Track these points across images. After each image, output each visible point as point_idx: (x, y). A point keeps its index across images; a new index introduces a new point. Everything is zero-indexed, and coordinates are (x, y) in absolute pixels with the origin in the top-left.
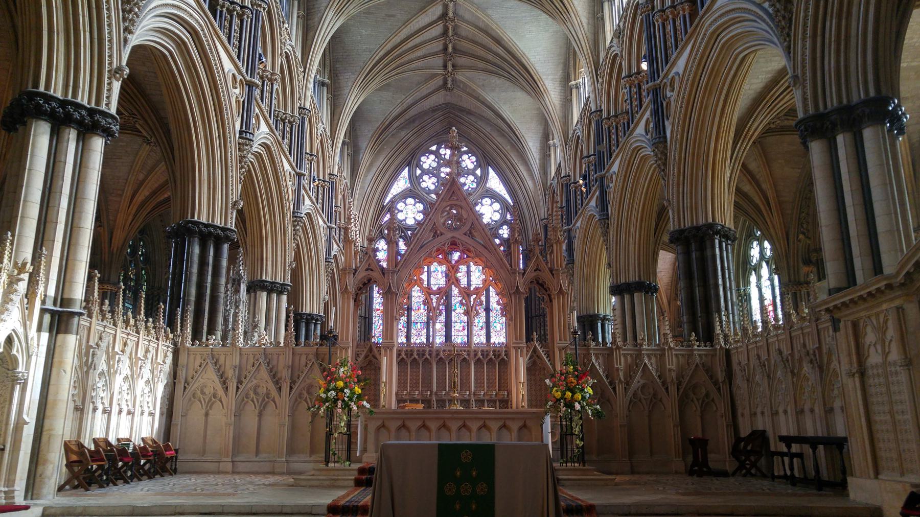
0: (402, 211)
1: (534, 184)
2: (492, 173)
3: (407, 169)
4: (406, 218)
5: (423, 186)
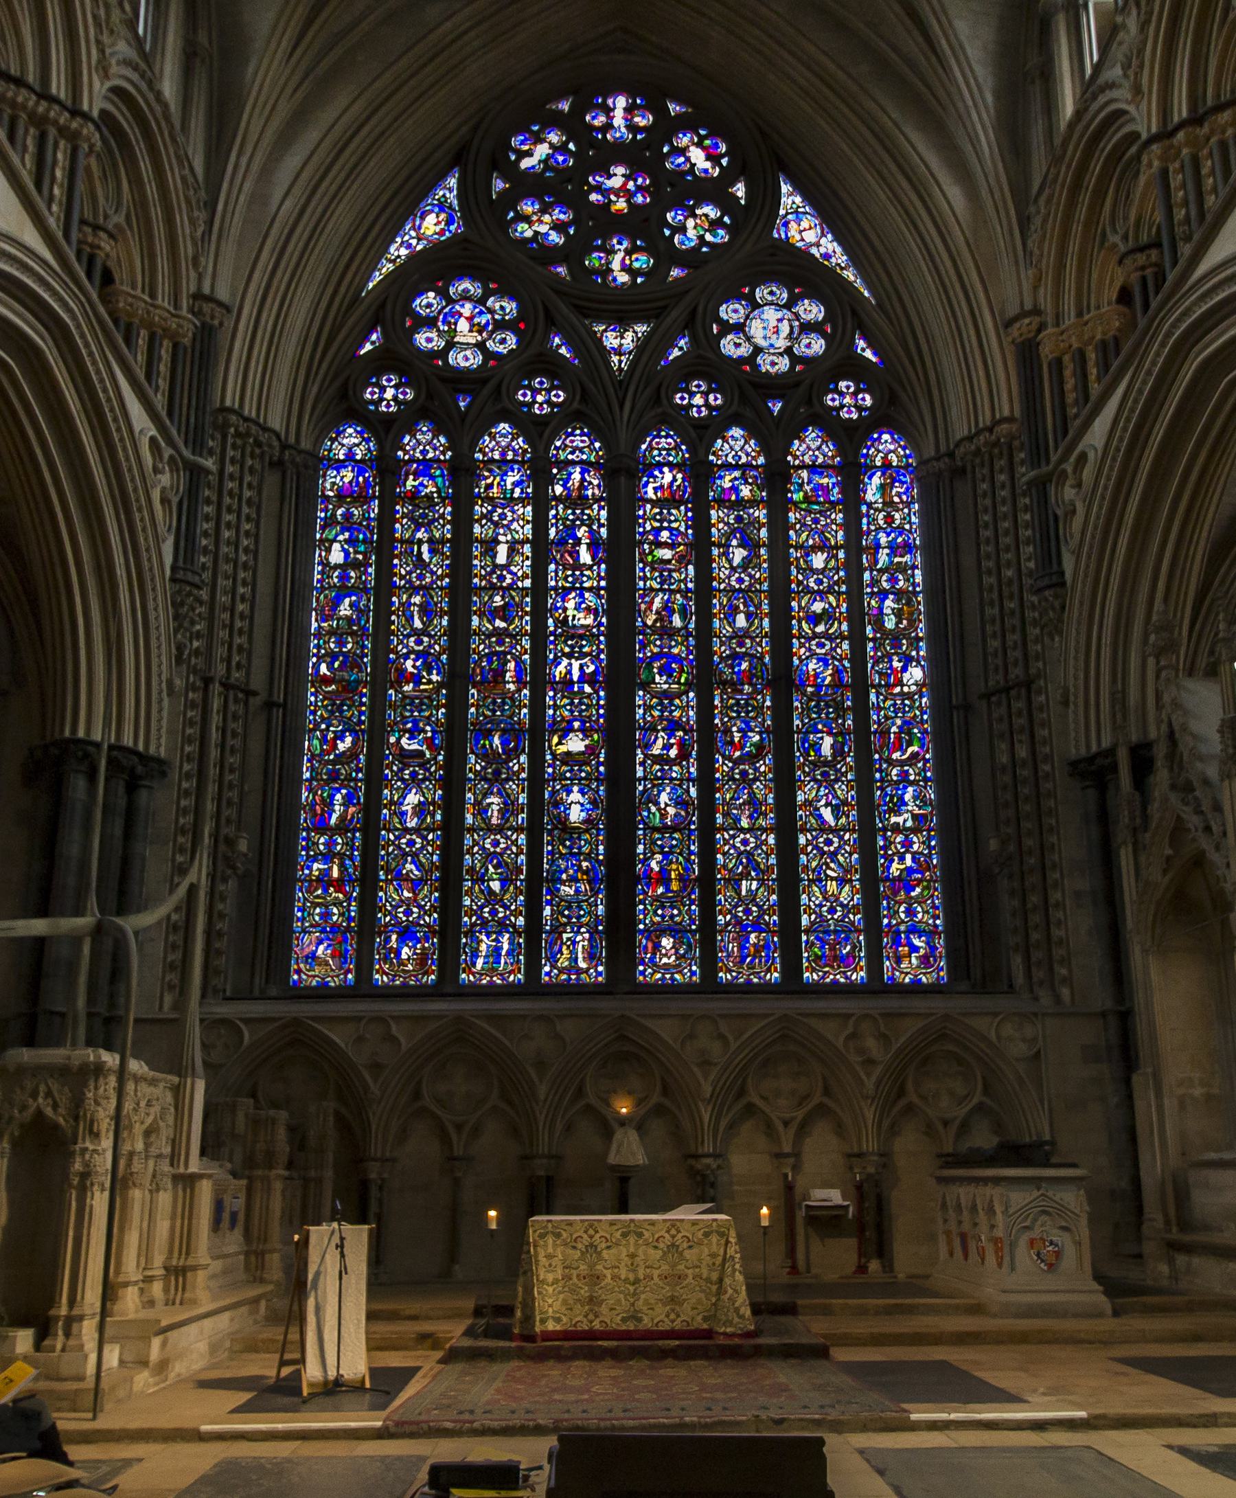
1: (972, 194)
2: (789, 198)
4: (450, 345)
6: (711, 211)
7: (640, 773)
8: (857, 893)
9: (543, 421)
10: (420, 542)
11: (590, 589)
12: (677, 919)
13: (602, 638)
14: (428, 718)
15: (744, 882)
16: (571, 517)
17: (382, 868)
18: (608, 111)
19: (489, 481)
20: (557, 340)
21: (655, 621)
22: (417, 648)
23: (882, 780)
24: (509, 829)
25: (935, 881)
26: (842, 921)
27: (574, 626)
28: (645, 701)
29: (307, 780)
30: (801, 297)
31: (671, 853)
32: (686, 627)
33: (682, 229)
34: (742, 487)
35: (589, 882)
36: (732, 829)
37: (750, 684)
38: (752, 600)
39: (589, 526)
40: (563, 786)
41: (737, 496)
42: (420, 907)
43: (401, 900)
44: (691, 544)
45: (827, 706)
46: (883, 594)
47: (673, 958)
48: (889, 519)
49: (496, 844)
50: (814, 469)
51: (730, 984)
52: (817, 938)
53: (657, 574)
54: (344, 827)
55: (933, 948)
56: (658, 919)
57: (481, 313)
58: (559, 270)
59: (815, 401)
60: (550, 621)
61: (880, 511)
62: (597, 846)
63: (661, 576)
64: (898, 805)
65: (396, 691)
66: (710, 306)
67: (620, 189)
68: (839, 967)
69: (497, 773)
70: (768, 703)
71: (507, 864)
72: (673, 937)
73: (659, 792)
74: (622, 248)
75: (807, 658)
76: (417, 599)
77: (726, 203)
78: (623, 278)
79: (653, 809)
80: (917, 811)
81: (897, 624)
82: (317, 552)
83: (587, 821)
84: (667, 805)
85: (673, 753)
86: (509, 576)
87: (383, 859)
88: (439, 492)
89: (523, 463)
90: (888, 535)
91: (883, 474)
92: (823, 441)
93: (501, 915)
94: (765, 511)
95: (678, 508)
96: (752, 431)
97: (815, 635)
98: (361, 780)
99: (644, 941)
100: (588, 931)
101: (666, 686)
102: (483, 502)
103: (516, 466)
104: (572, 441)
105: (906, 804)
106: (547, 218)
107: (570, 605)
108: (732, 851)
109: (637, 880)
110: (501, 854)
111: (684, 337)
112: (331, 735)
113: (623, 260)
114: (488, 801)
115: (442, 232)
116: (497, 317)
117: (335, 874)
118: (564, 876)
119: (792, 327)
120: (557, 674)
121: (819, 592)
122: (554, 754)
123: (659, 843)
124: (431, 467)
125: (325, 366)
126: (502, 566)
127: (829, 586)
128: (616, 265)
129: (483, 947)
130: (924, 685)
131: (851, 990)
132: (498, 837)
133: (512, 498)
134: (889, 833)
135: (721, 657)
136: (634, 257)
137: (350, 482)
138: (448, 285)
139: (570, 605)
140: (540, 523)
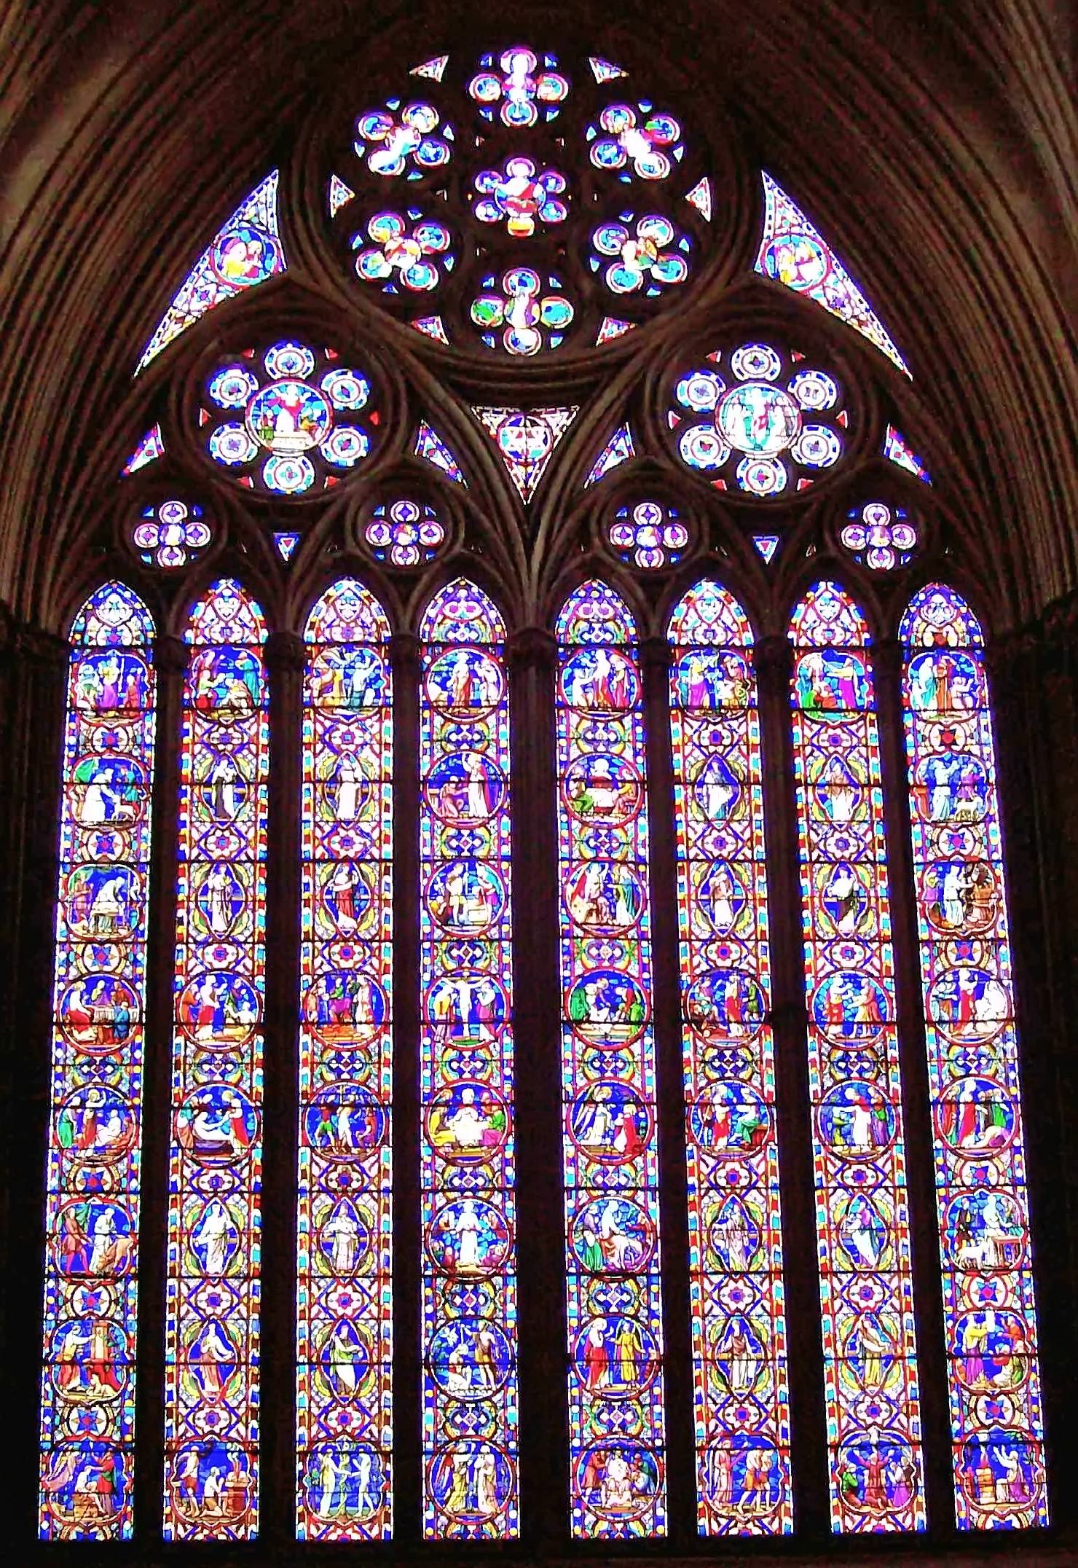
0: (236, 417)
3: (269, 190)
4: (265, 454)
5: (365, 274)
6: (658, 231)
7: (569, 1181)
8: (913, 1378)
9: (406, 577)
10: (221, 782)
11: (486, 860)
12: (633, 1430)
13: (505, 944)
14: (236, 1085)
15: (736, 1363)
16: (454, 737)
17: (171, 1345)
18: (502, 76)
19: (327, 678)
20: (429, 443)
21: (590, 913)
22: (217, 965)
23: (948, 1185)
24: (364, 1276)
25: (1031, 1356)
26: (889, 1427)
27: (462, 924)
28: (574, 1052)
29: (53, 1192)
30: (802, 368)
31: (620, 1315)
32: (638, 924)
33: (619, 259)
34: (719, 685)
35: (493, 1367)
36: (716, 1273)
37: (741, 1022)
38: (740, 879)
39: (483, 753)
40: (449, 1201)
41: (712, 698)
42: (231, 1410)
43: (202, 1399)
44: (643, 782)
45: (860, 1058)
46: (943, 866)
47: (627, 1495)
48: (948, 738)
49: (345, 1302)
50: (829, 652)
51: (715, 1538)
52: (851, 1457)
53: (589, 832)
54: (109, 1277)
55: (1027, 1470)
56: (601, 1430)
57: (312, 399)
58: (430, 327)
59: (827, 537)
60: (424, 914)
61: (934, 724)
62: (504, 1304)
63: (597, 836)
64: (970, 1228)
65: (187, 1039)
66: (663, 382)
67: (522, 197)
68: (886, 1505)
69: (345, 1180)
70: (768, 1055)
71: (364, 1338)
72: (625, 1459)
73: (599, 1215)
74: (528, 290)
75: (828, 975)
76: (217, 881)
77: (682, 217)
78: (528, 340)
79: (591, 1239)
80: (1001, 1236)
81: (966, 916)
82: (66, 802)
83: (489, 1262)
84: (613, 1233)
85: (621, 1142)
86: (358, 839)
87: (171, 1327)
88: (249, 698)
89: (378, 644)
90: (948, 763)
91: (936, 662)
92: (843, 606)
93: (355, 1424)
94: (756, 724)
95: (620, 720)
96: (735, 587)
97: (838, 939)
98: (135, 1192)
99: (581, 1467)
100: (492, 1451)
101: (606, 1028)
102: (316, 712)
103: (368, 652)
104: (454, 610)
105: (983, 1224)
106: (410, 245)
107: (456, 887)
108: (717, 1311)
109: (568, 1361)
110: (354, 1319)
111: (624, 434)
112: (88, 1115)
113: (529, 308)
114: (332, 1227)
115: (253, 273)
116: (337, 405)
117: (99, 1352)
118: (454, 1358)
119: (787, 417)
120: (436, 1007)
121: (842, 863)
122: (435, 1151)
123: (602, 1298)
124: (235, 656)
125: (76, 493)
126: (348, 823)
127: (859, 853)
128: (518, 320)
129: (329, 1481)
130: (1007, 1021)
131: (902, 1542)
132: (349, 1289)
133: (361, 706)
134: (959, 1276)
135: (694, 977)
136: (545, 303)
137: (115, 685)
138: (263, 351)
139: (456, 887)
140: (406, 748)
